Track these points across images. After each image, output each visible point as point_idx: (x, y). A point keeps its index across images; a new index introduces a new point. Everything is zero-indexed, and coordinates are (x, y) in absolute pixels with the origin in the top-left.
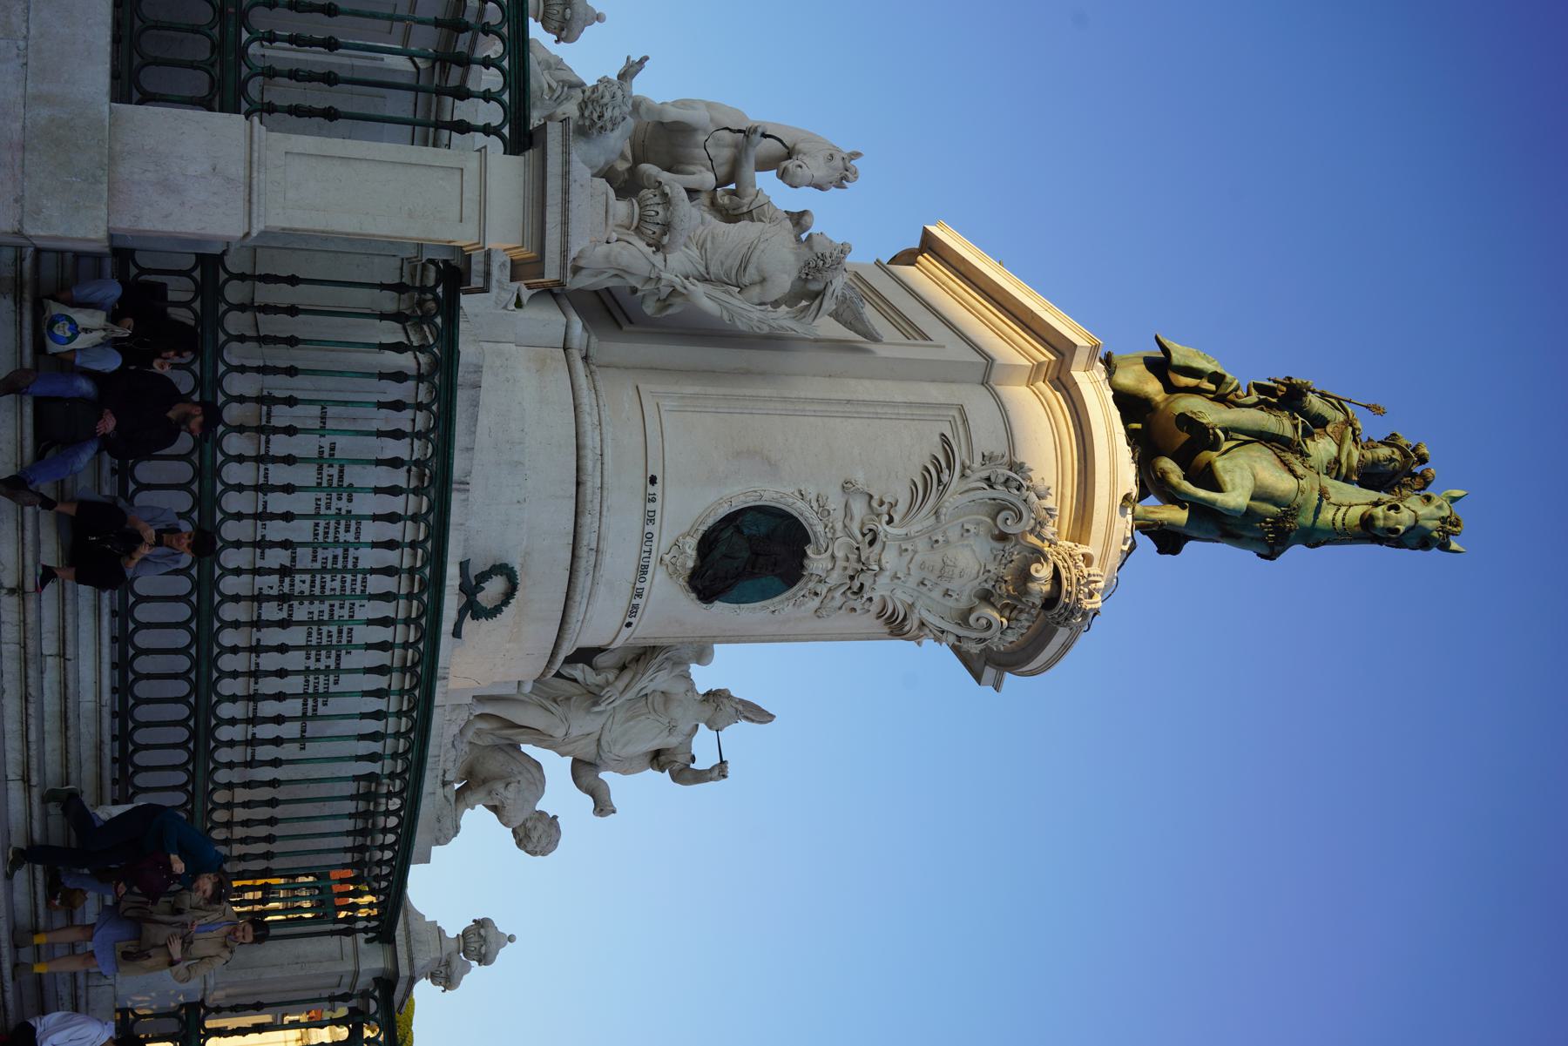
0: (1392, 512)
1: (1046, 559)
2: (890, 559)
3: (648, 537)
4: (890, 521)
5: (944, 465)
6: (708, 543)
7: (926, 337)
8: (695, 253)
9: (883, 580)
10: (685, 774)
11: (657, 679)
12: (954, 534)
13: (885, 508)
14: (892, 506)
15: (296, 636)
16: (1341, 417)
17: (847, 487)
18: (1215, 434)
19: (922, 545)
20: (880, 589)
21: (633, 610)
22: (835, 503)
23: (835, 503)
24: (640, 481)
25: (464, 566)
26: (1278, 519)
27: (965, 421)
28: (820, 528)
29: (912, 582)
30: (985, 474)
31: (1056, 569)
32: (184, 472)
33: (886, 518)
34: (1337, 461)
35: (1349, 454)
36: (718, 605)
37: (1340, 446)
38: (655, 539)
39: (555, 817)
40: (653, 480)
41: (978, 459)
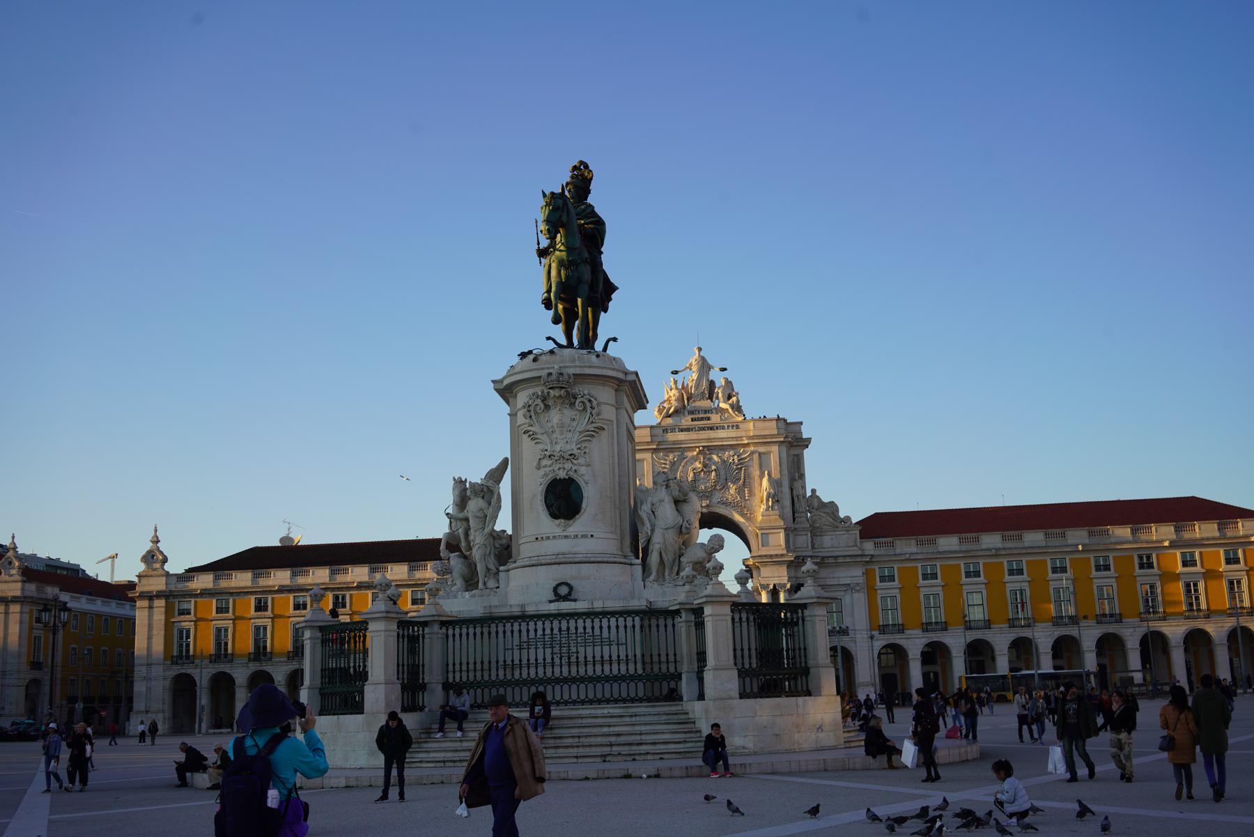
2: (558, 448)
6: (554, 516)
9: (568, 447)
11: (644, 511)
12: (550, 425)
15: (581, 650)
17: (538, 468)
19: (554, 436)
20: (573, 447)
21: (584, 536)
22: (542, 472)
23: (542, 472)
24: (537, 543)
25: (551, 602)
26: (566, 269)
29: (570, 435)
32: (509, 689)
36: (584, 505)
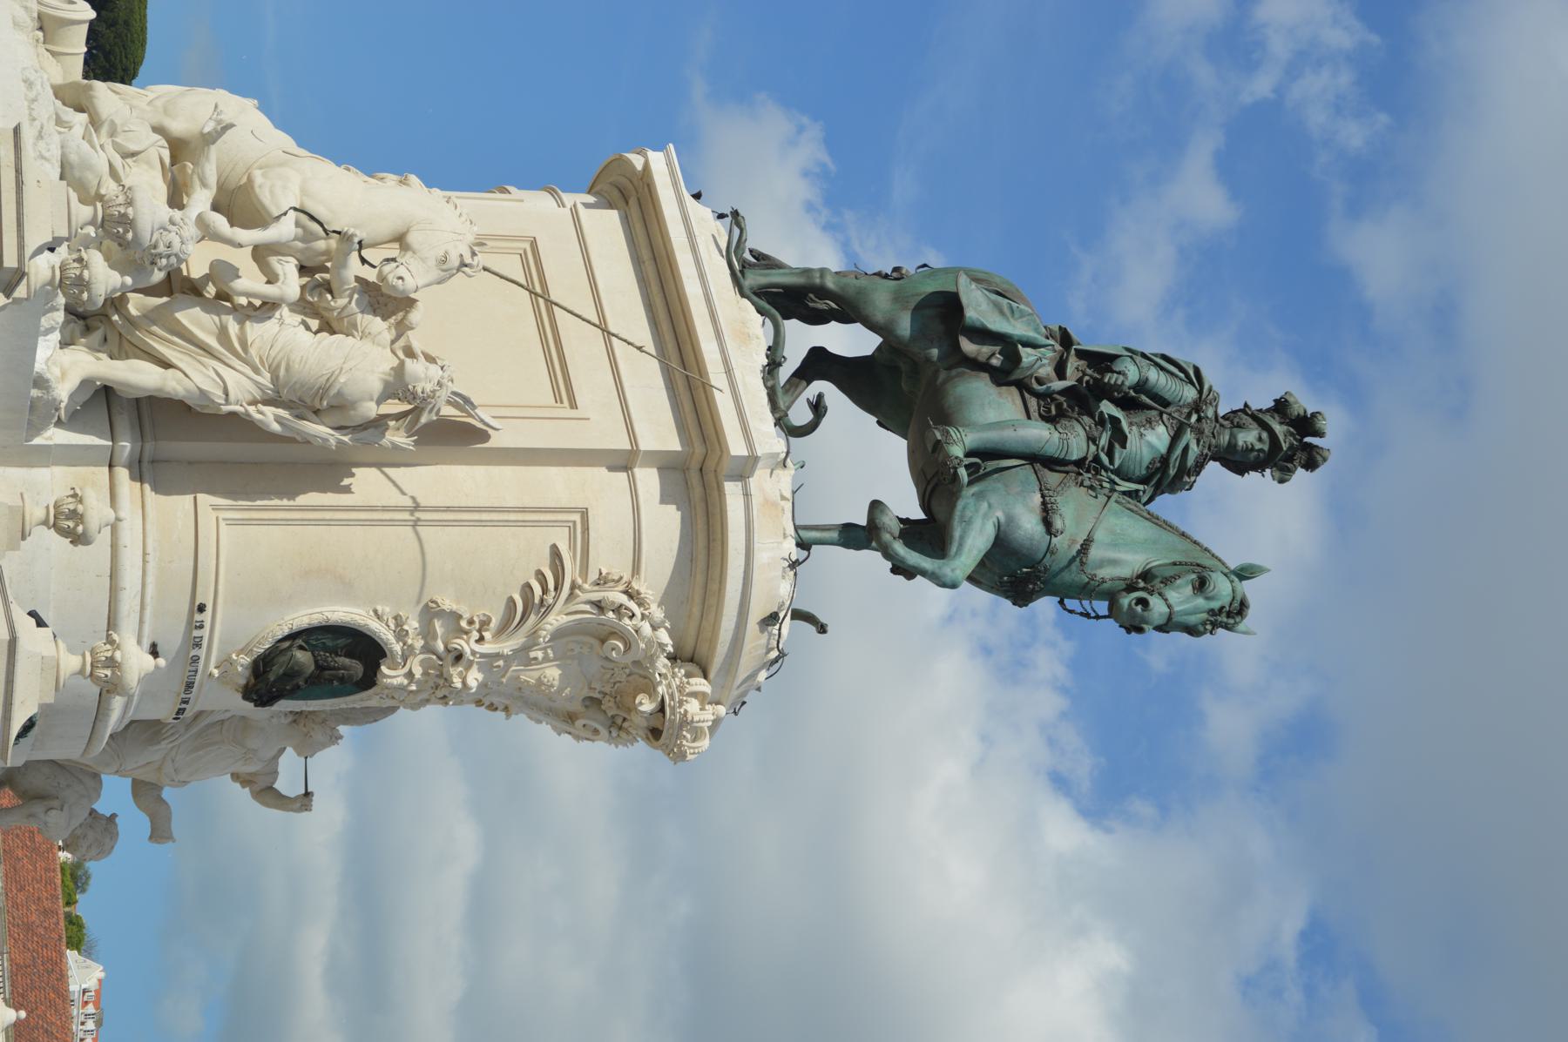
0: (1139, 608)
1: (655, 689)
3: (196, 659)
4: (481, 639)
5: (551, 585)
6: (262, 665)
7: (573, 405)
8: (265, 379)
10: (267, 794)
13: (477, 626)
14: (485, 623)
16: (1190, 393)
18: (956, 476)
27: (586, 530)
28: (397, 647)
30: (596, 596)
31: (661, 709)
33: (475, 635)
34: (1165, 460)
35: (1186, 449)
37: (1175, 439)
38: (202, 661)
39: (114, 816)
40: (201, 608)
41: (593, 576)
